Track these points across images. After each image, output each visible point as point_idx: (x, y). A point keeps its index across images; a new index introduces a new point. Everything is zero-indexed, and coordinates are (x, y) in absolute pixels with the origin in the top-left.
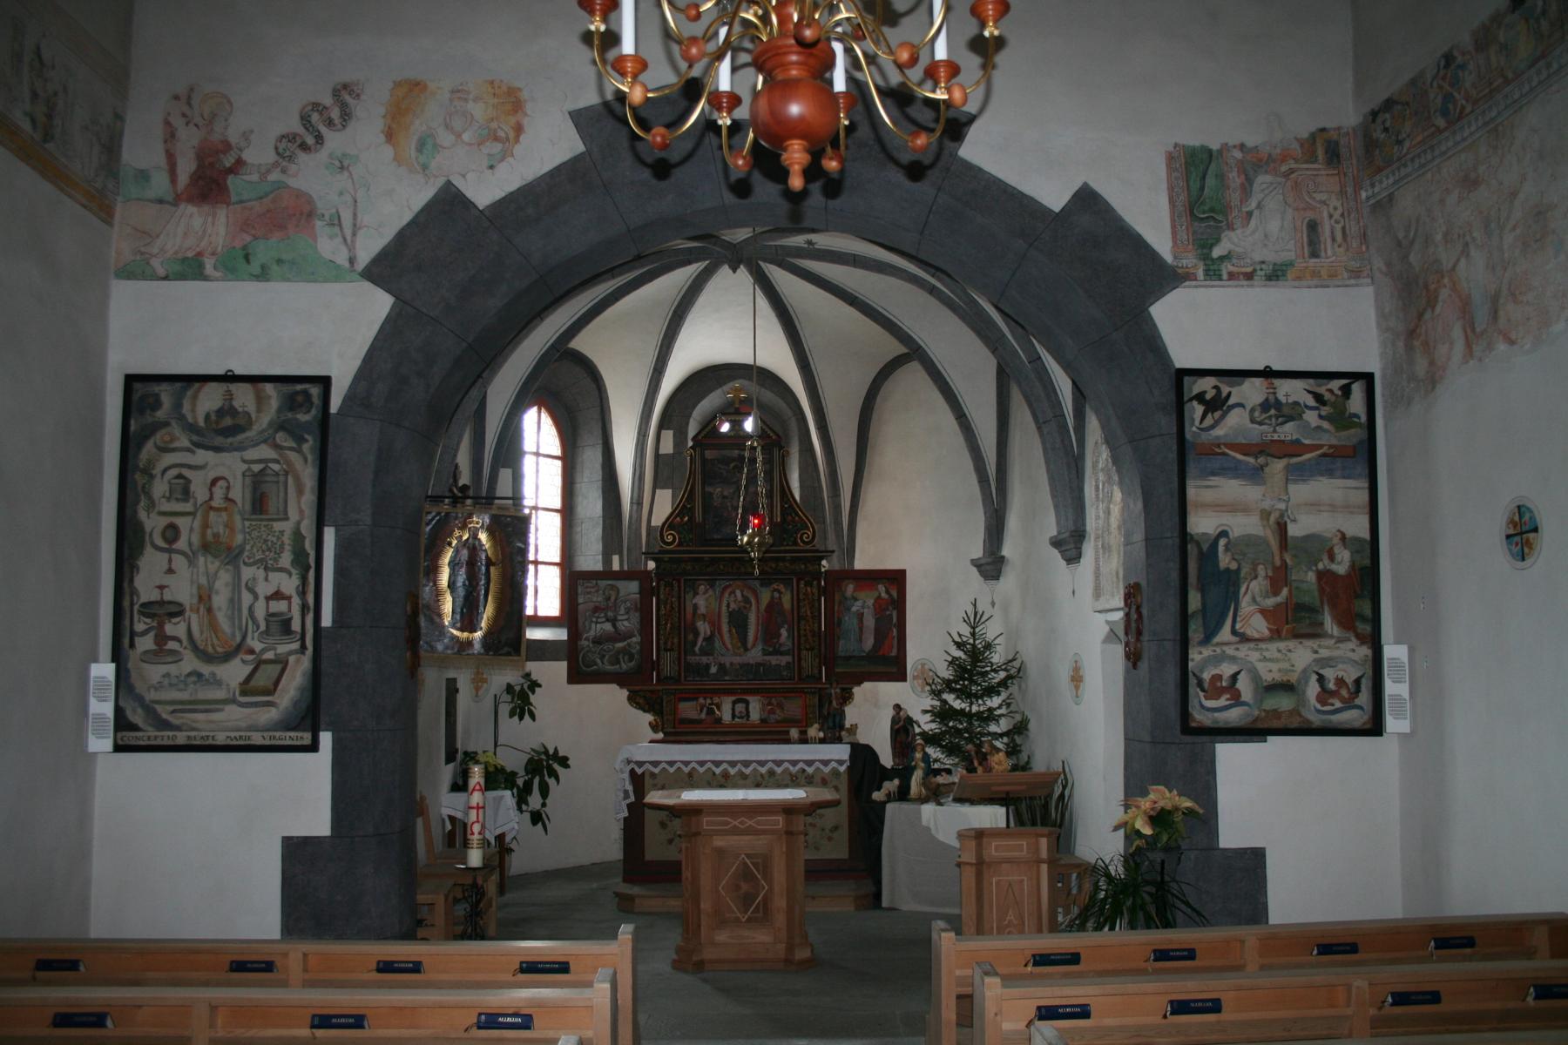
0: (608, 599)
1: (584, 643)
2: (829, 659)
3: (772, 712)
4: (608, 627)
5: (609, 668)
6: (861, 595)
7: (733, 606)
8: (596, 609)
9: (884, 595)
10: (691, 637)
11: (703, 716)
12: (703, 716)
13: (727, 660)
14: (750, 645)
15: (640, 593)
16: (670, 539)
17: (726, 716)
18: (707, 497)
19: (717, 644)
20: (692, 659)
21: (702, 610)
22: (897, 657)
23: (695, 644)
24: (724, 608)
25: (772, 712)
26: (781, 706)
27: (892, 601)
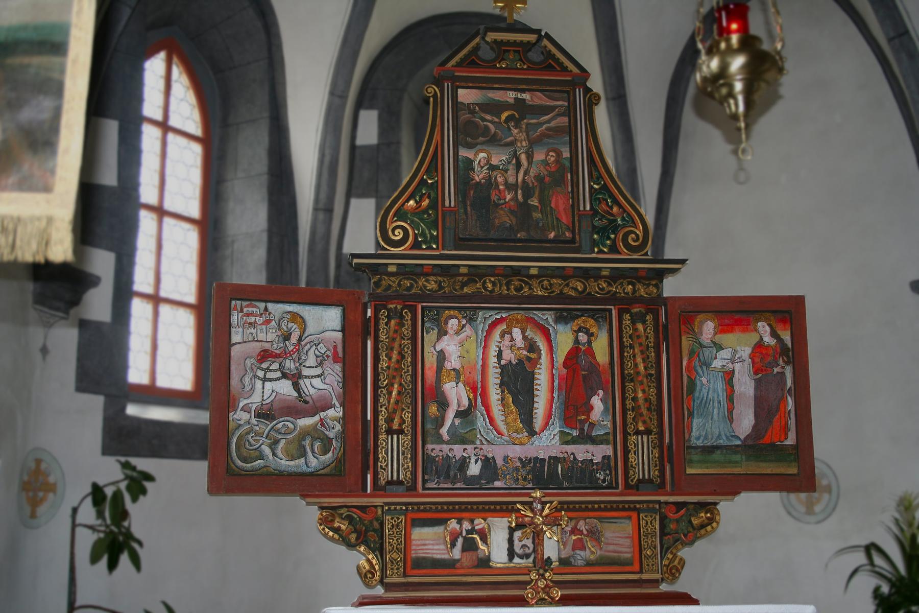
0: (287, 337)
1: (239, 416)
2: (673, 452)
3: (579, 545)
4: (285, 388)
5: (285, 464)
6: (728, 339)
7: (509, 356)
8: (265, 355)
9: (768, 340)
10: (433, 409)
11: (457, 553)
12: (457, 553)
13: (498, 452)
14: (538, 424)
15: (343, 330)
16: (398, 235)
17: (498, 553)
18: (464, 168)
19: (481, 422)
20: (436, 450)
21: (453, 362)
22: (796, 447)
23: (440, 422)
24: (492, 360)
25: (579, 545)
26: (594, 534)
27: (783, 350)
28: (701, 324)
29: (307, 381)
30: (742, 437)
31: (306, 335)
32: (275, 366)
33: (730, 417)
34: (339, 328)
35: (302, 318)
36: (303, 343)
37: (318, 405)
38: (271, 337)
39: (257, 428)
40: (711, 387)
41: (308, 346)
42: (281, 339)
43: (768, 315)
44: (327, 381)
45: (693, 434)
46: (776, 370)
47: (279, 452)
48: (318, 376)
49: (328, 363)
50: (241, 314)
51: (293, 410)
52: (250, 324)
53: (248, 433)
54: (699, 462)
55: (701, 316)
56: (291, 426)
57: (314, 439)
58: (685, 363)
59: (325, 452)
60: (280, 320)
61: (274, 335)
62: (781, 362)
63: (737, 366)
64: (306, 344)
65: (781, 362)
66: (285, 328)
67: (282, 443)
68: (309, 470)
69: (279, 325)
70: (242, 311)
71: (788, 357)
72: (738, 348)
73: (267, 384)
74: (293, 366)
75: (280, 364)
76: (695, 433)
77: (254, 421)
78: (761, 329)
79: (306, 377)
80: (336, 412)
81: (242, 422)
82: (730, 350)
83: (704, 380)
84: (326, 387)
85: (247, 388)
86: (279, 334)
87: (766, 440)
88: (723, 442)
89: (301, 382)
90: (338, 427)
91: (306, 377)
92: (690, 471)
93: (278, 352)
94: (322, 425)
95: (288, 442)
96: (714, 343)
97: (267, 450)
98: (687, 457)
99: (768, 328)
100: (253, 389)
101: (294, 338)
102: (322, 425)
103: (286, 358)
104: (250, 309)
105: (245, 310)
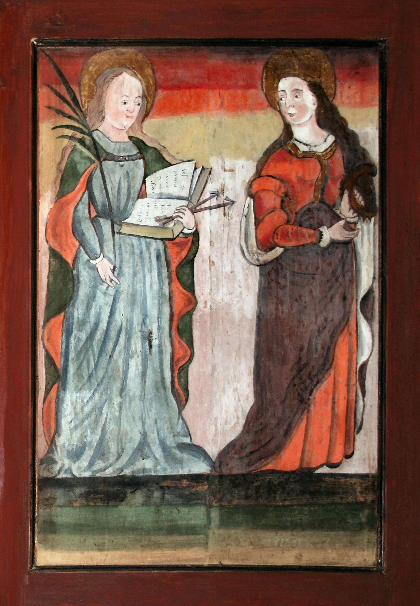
6: (181, 132)
9: (310, 135)
28: (100, 82)
30: (213, 451)
33: (180, 389)
40: (125, 284)
43: (314, 52)
45: (62, 440)
46: (329, 234)
54: (78, 528)
55: (104, 56)
58: (45, 207)
62: (345, 208)
63: (209, 221)
65: (345, 208)
71: (367, 193)
72: (214, 163)
76: (66, 439)
78: (287, 102)
82: (189, 167)
83: (104, 266)
87: (288, 460)
88: (152, 465)
92: (46, 557)
96: (140, 145)
98: (41, 513)
99: (309, 99)
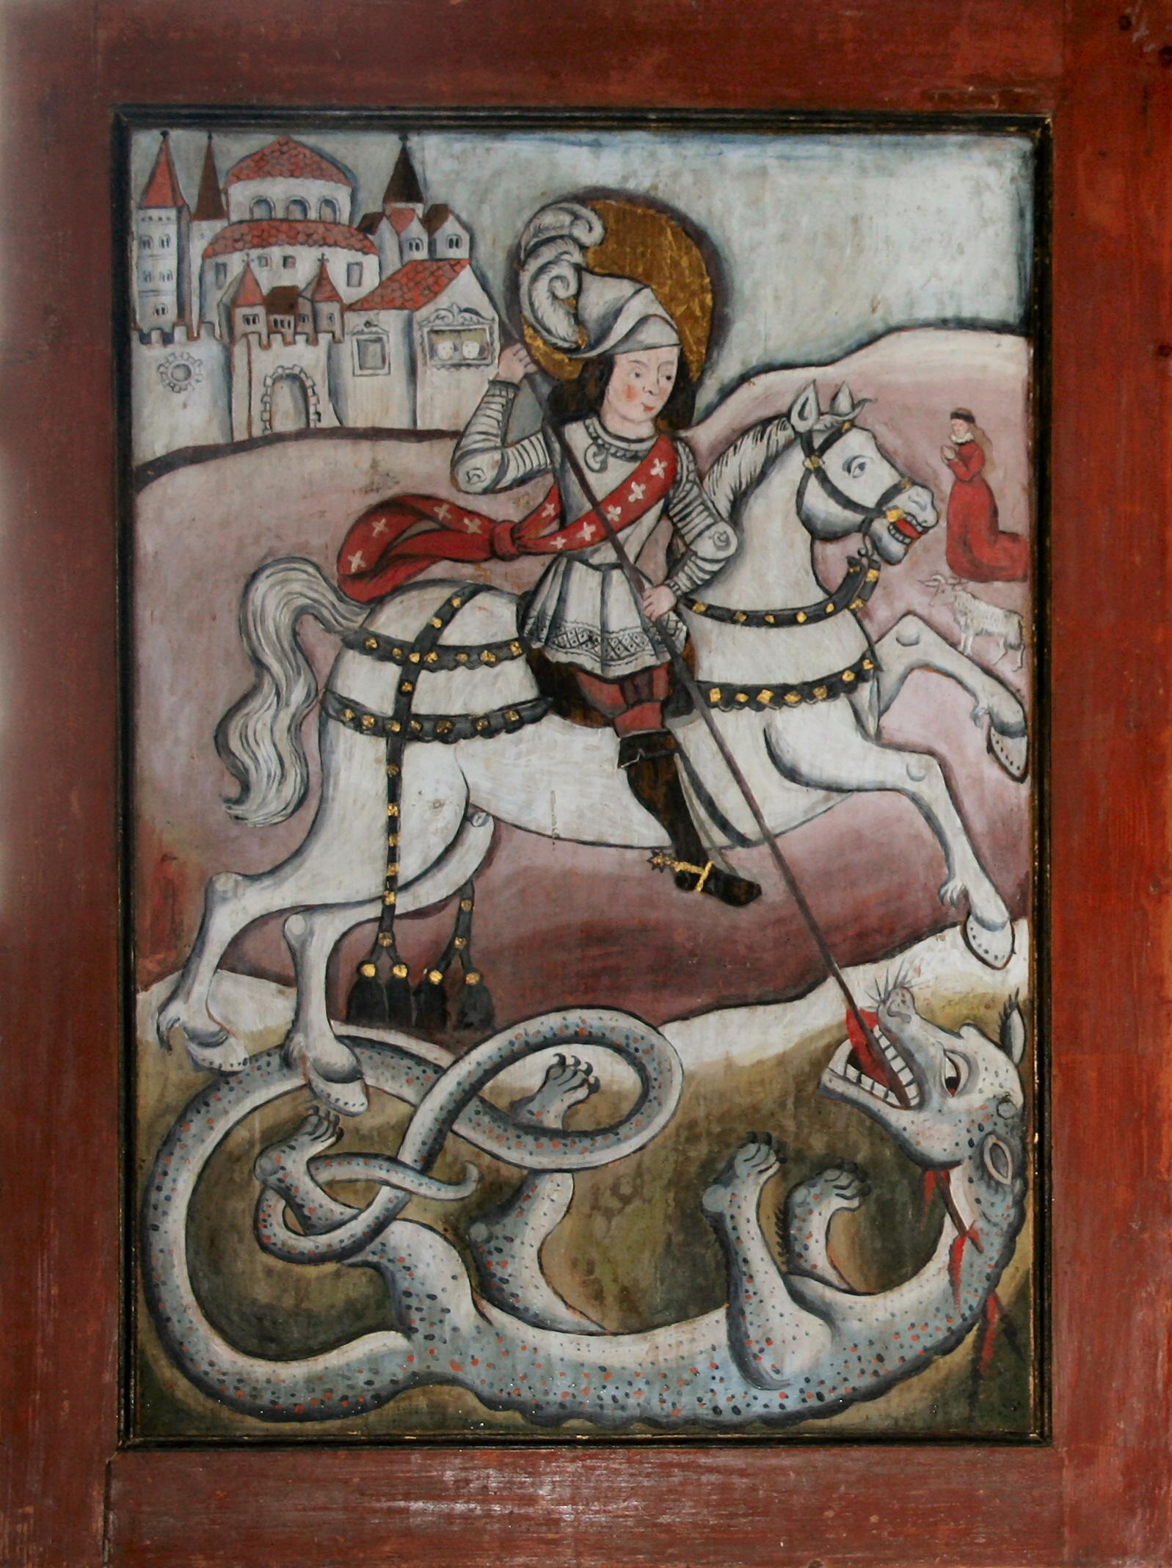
0: (574, 390)
1: (213, 1010)
4: (569, 784)
8: (401, 541)
15: (1035, 322)
29: (740, 728)
31: (728, 366)
32: (486, 620)
34: (999, 293)
35: (695, 235)
36: (705, 434)
37: (830, 906)
38: (451, 394)
39: (350, 1097)
41: (749, 454)
42: (529, 409)
44: (899, 722)
47: (522, 1271)
48: (833, 686)
49: (906, 586)
50: (205, 231)
51: (621, 960)
52: (283, 301)
53: (281, 1136)
56: (615, 1073)
57: (798, 1169)
59: (890, 1262)
60: (517, 259)
61: (474, 383)
64: (731, 442)
66: (560, 325)
67: (547, 1210)
68: (764, 1402)
69: (511, 299)
70: (212, 205)
73: (424, 760)
74: (623, 618)
75: (525, 603)
77: (324, 1042)
79: (732, 696)
80: (975, 964)
81: (232, 1056)
84: (892, 767)
85: (270, 800)
86: (515, 365)
89: (692, 736)
90: (997, 1076)
91: (732, 696)
93: (504, 509)
94: (866, 1060)
95: (597, 1199)
97: (429, 1260)
100: (311, 802)
101: (635, 397)
102: (866, 1060)
103: (575, 554)
104: (279, 189)
105: (240, 196)
